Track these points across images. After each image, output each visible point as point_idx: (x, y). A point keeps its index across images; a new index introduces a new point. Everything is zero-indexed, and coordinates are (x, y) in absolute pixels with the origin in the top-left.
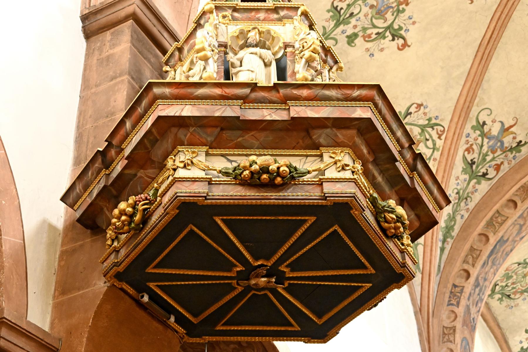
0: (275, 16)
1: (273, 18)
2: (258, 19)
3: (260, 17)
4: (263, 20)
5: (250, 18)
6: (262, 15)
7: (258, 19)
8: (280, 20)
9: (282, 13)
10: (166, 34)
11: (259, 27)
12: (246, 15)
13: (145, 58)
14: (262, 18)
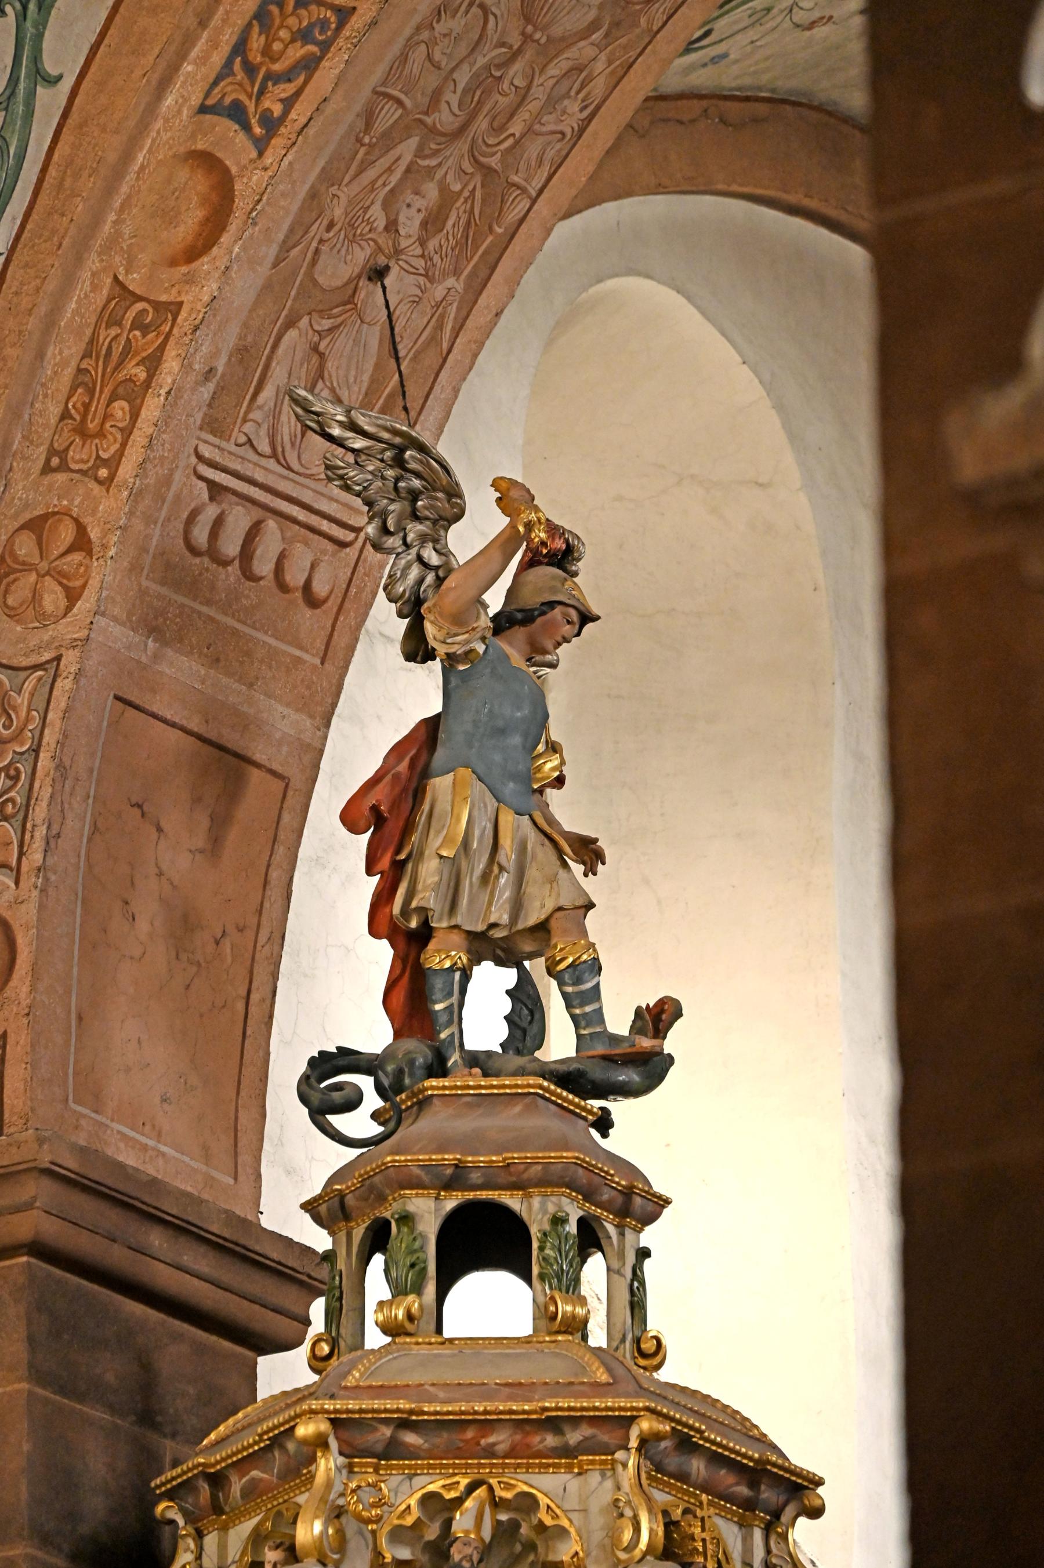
0: (551, 1440)
1: (541, 1446)
2: (490, 1452)
3: (494, 1444)
4: (506, 1456)
5: (459, 1448)
6: (500, 1439)
7: (490, 1452)
8: (567, 1452)
9: (573, 1437)
10: (157, 1239)
11: (493, 1481)
12: (442, 1439)
13: (81, 1398)
14: (501, 1448)
